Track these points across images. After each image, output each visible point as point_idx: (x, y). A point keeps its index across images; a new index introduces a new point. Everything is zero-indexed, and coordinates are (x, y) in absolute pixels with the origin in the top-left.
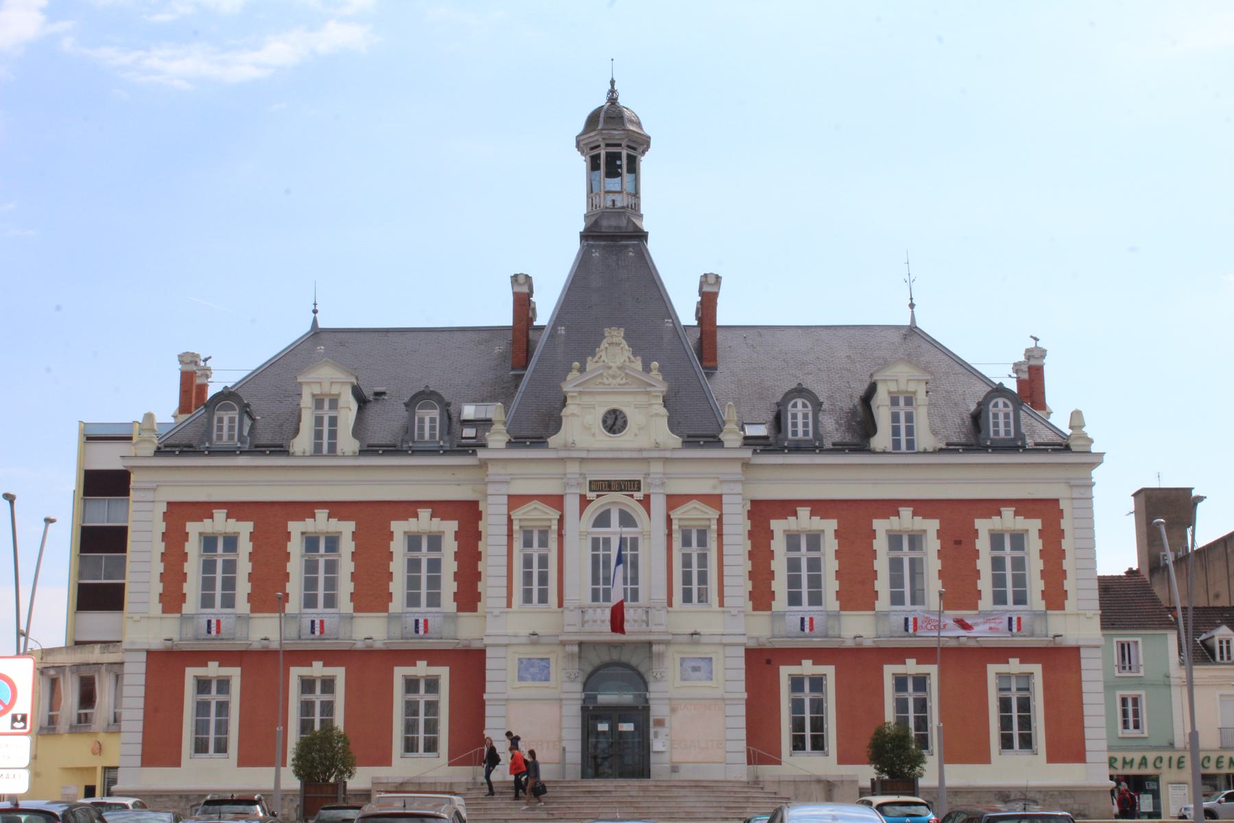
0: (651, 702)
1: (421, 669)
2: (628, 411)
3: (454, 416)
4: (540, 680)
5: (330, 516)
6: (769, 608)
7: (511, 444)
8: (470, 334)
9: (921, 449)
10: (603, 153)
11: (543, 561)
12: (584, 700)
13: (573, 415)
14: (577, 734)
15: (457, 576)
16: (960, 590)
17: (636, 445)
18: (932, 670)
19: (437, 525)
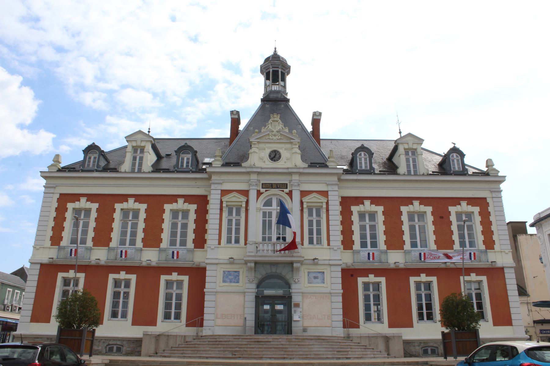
0: (293, 294)
1: (175, 276)
2: (282, 152)
3: (200, 160)
4: (234, 282)
5: (135, 201)
6: (351, 248)
7: (223, 165)
8: (215, 141)
9: (421, 173)
10: (271, 70)
11: (238, 224)
12: (257, 293)
13: (255, 152)
14: (253, 311)
15: (195, 231)
16: (444, 241)
17: (286, 166)
18: (434, 279)
19: (187, 206)
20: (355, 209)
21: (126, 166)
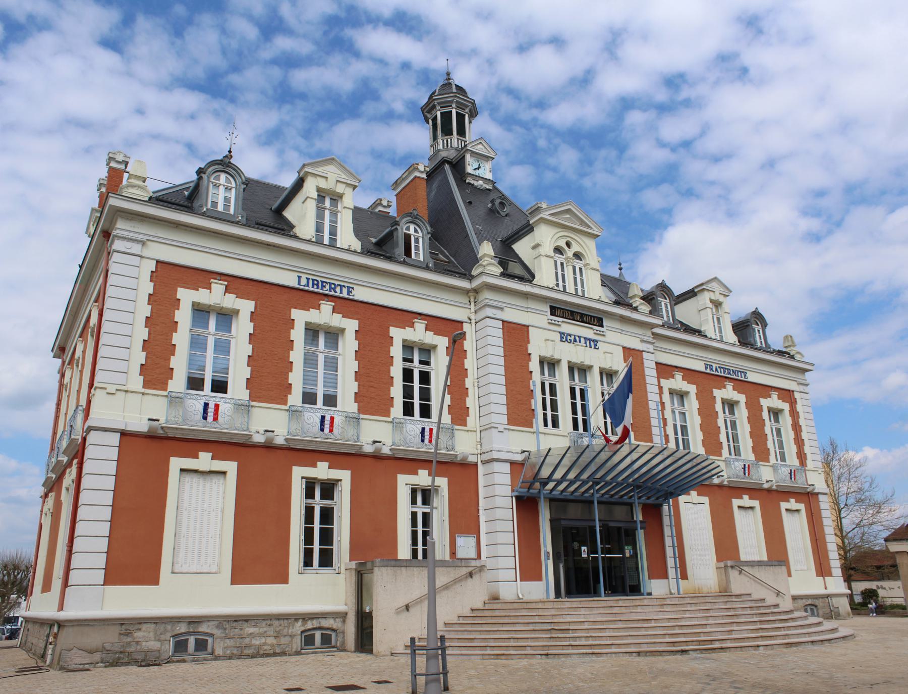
18: (344, 476)
20: (187, 296)
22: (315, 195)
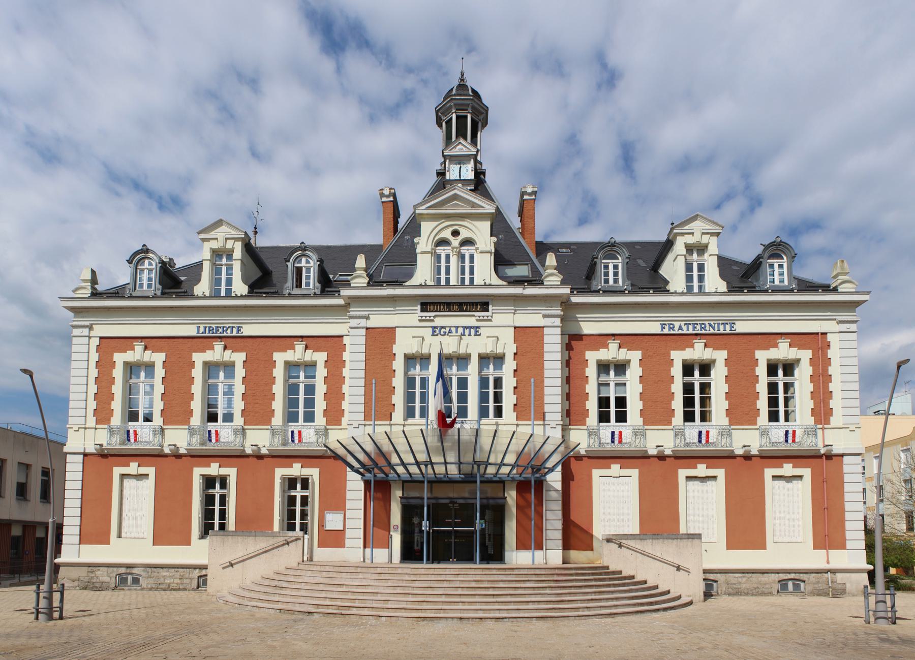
7: (369, 284)
21: (203, 287)
22: (684, 252)
